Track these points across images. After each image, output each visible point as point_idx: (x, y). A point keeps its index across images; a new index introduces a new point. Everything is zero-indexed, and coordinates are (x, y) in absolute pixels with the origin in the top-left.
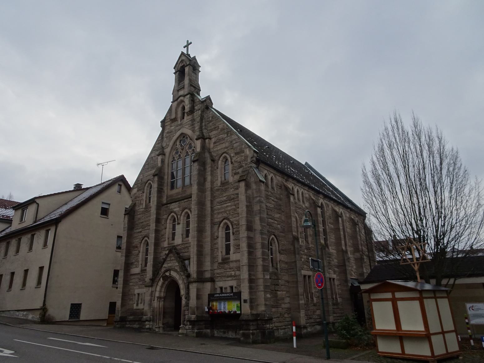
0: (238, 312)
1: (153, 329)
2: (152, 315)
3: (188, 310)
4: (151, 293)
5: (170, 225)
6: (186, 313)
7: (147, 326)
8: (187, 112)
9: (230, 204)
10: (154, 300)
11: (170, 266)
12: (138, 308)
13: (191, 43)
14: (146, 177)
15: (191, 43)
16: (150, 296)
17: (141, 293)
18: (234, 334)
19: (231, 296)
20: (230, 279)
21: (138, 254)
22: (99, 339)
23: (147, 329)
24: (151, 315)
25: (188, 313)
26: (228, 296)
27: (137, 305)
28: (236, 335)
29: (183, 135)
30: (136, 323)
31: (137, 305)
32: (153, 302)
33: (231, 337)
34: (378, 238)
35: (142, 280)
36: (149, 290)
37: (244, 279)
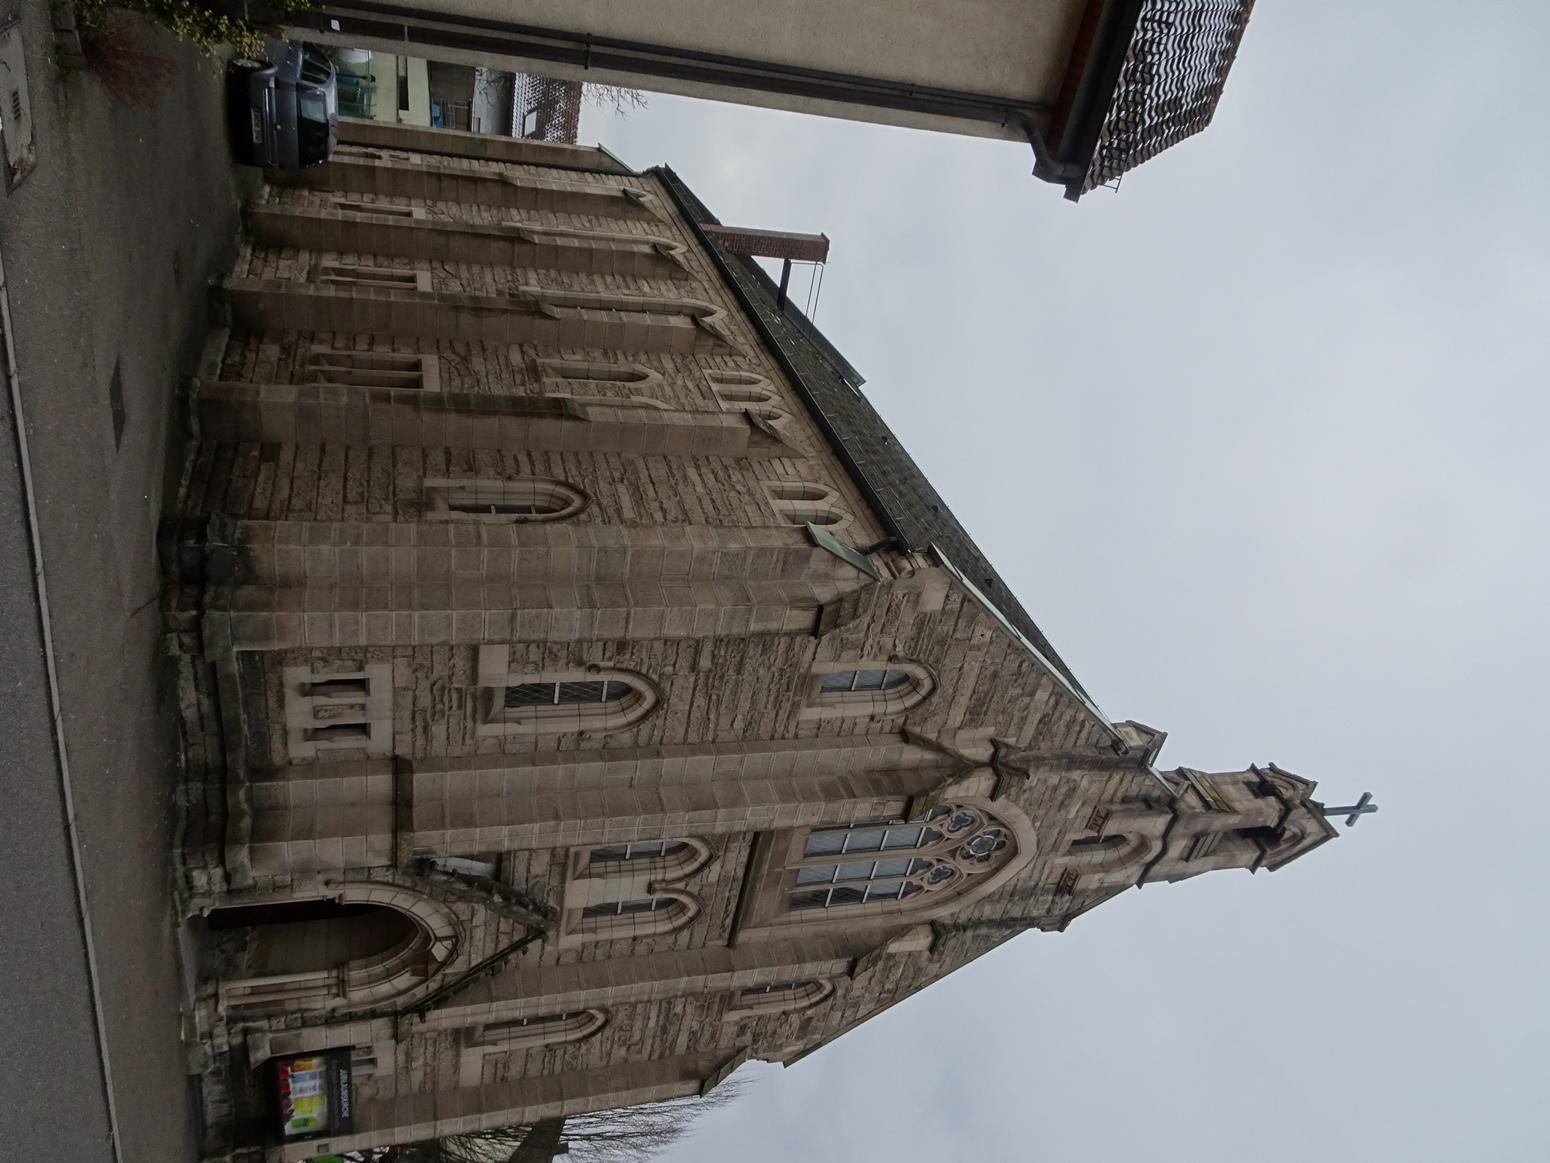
0: (289, 1129)
1: (191, 897)
2: (255, 886)
3: (288, 1028)
4: (363, 868)
5: (640, 920)
6: (274, 1022)
7: (200, 879)
8: (1074, 880)
9: (652, 1023)
10: (327, 883)
11: (471, 938)
12: (291, 695)
13: (1373, 809)
14: (961, 668)
15: (1373, 809)
16: (346, 863)
17: (369, 707)
18: (218, 1098)
19: (340, 1113)
20: (401, 1058)
21: (580, 663)
22: (86, 955)
23: (188, 879)
24: (256, 883)
25: (278, 1031)
26: (340, 1107)
27: (309, 690)
28: (214, 1102)
29: (1008, 849)
30: (206, 702)
31: (309, 690)
32: (321, 878)
33: (205, 1091)
34: (517, 888)
35: (439, 707)
36: (377, 853)
37: (393, 1134)
